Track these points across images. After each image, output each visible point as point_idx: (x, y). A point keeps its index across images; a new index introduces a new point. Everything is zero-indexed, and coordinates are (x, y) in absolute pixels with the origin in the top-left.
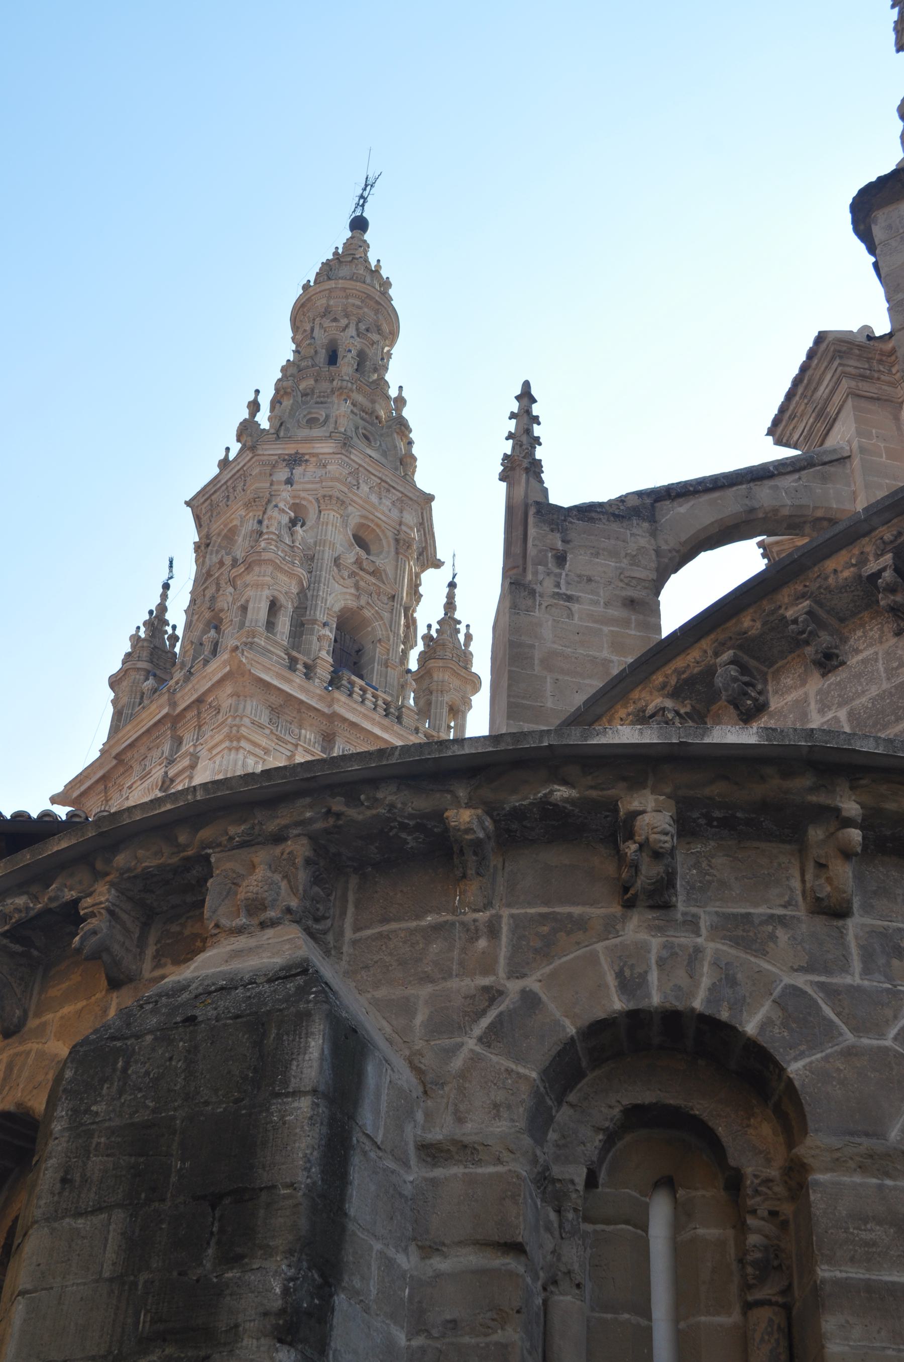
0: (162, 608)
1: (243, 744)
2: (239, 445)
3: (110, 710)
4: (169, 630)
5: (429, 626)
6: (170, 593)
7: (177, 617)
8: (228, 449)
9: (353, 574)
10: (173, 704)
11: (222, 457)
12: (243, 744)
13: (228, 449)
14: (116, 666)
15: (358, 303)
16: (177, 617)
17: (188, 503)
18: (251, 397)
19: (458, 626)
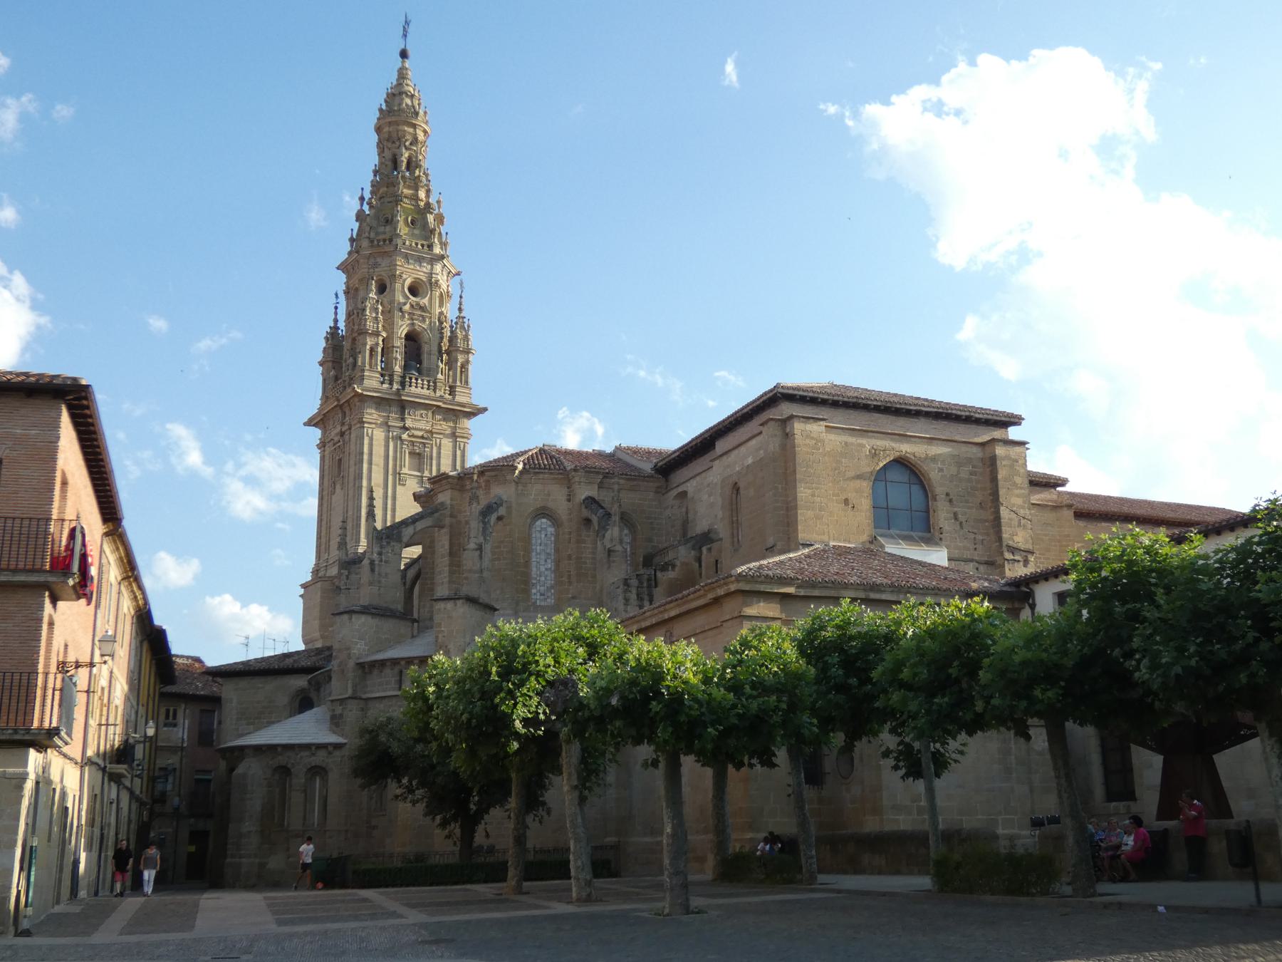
0: (336, 321)
1: (366, 425)
2: (357, 224)
3: (321, 378)
4: (340, 331)
5: (452, 321)
6: (338, 310)
7: (342, 325)
8: (352, 230)
10: (338, 400)
11: (349, 236)
12: (366, 425)
13: (352, 230)
14: (320, 356)
16: (342, 325)
17: (338, 268)
18: (360, 195)
19: (465, 320)
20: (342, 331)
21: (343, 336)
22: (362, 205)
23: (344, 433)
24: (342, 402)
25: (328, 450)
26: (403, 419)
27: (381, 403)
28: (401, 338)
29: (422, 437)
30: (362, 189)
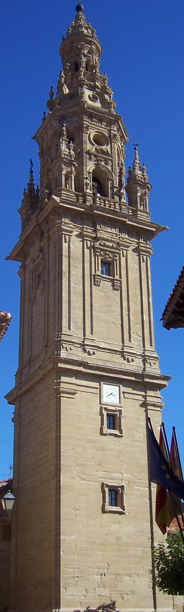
4: (36, 187)
7: (37, 182)
8: (45, 113)
9: (95, 156)
13: (45, 113)
14: (19, 205)
15: (84, 43)
16: (37, 182)
17: (33, 138)
20: (38, 186)
21: (38, 191)
22: (52, 97)
23: (43, 248)
24: (40, 221)
25: (28, 271)
26: (95, 231)
27: (76, 217)
28: (89, 173)
29: (112, 247)
30: (52, 87)
